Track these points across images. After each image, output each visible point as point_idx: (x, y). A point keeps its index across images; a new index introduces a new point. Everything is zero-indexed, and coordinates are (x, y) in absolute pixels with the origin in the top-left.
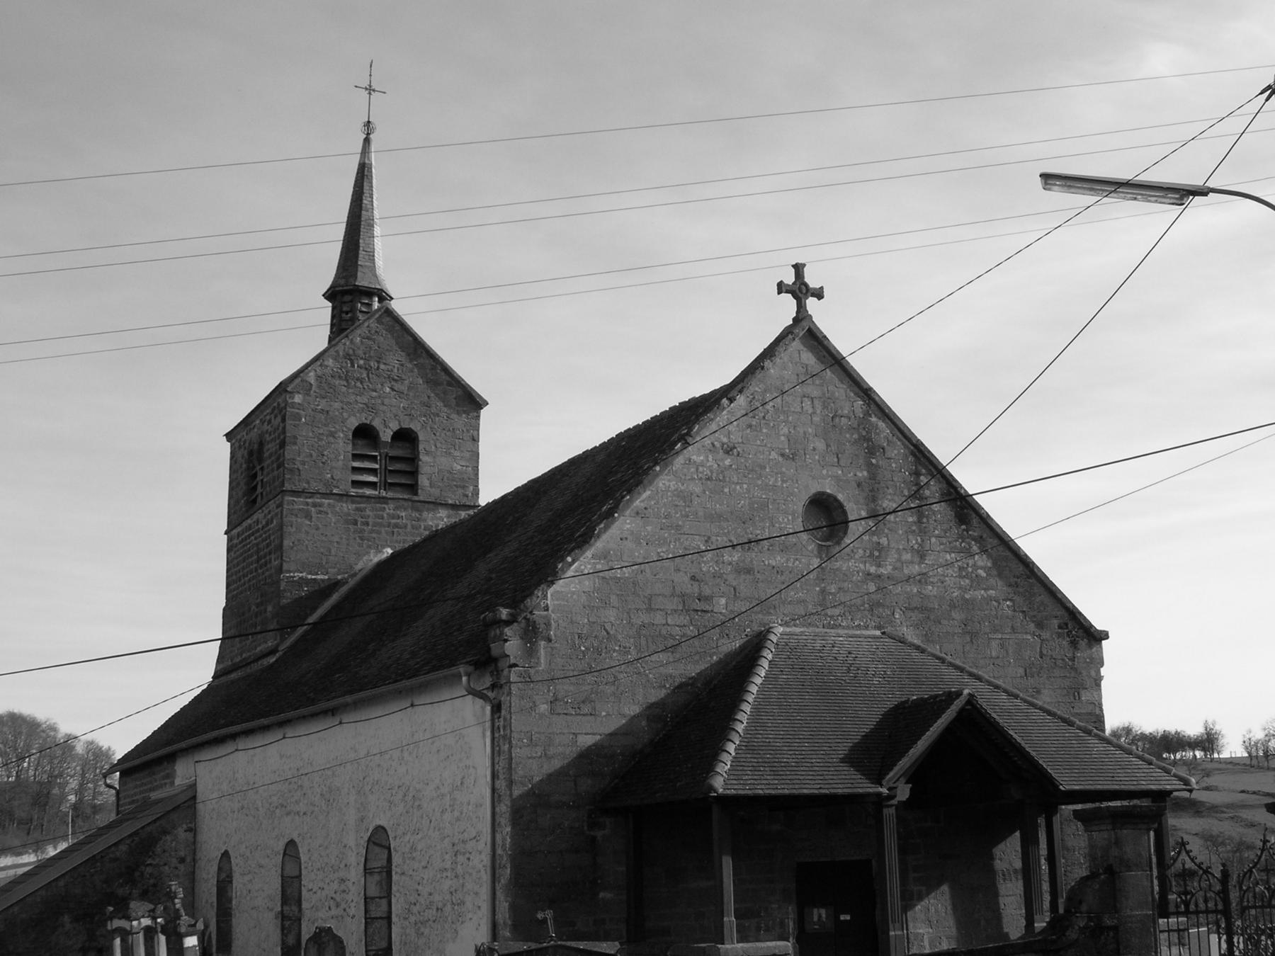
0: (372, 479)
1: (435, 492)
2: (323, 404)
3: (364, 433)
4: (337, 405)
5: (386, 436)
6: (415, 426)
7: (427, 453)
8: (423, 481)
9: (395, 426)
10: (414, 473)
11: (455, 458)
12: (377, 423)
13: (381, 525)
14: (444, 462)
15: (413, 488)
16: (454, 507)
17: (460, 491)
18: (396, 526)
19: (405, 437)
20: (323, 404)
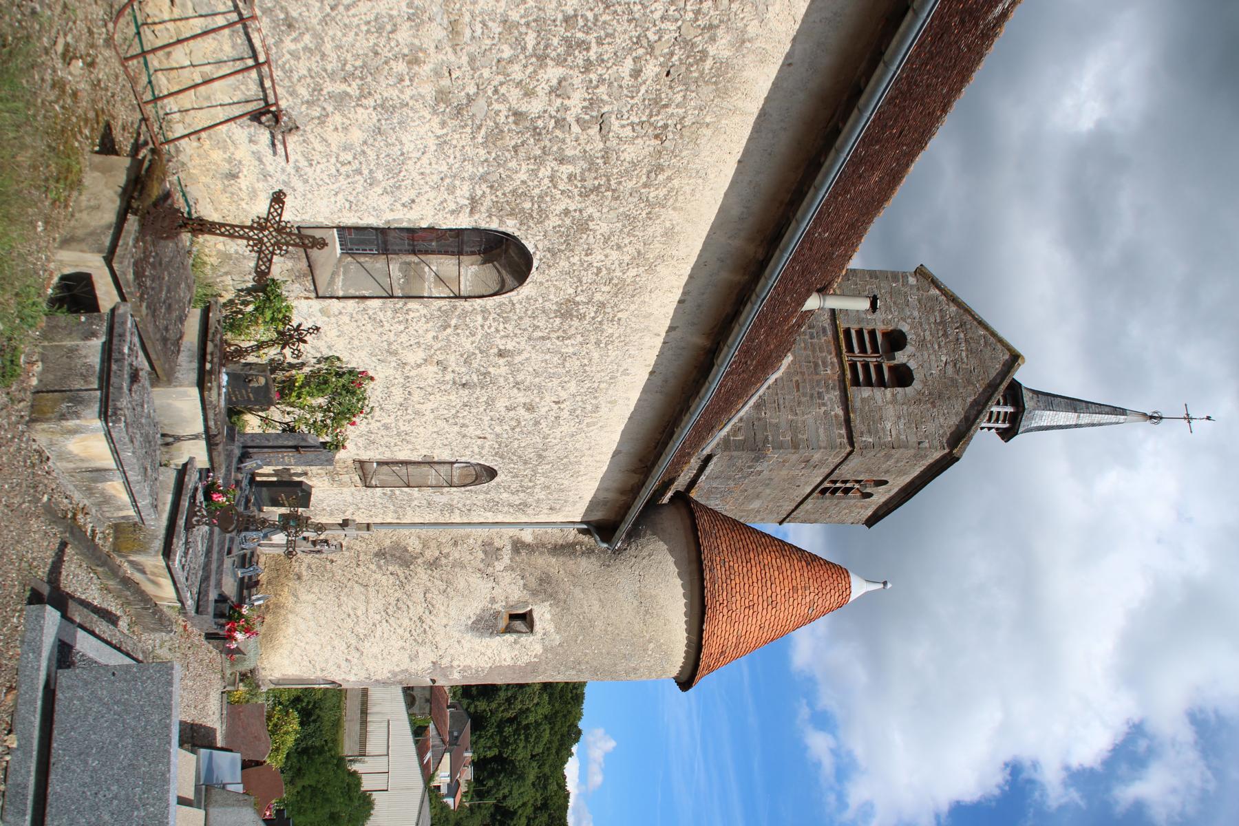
0: (856, 350)
1: (858, 404)
2: (913, 299)
3: (896, 340)
4: (916, 313)
5: (901, 357)
6: (917, 385)
7: (894, 395)
8: (866, 392)
9: (912, 365)
10: (869, 383)
11: (896, 423)
12: (909, 349)
13: (814, 351)
14: (890, 411)
15: (856, 382)
16: (848, 421)
17: (864, 429)
18: (816, 365)
19: (903, 377)
20: (913, 299)
